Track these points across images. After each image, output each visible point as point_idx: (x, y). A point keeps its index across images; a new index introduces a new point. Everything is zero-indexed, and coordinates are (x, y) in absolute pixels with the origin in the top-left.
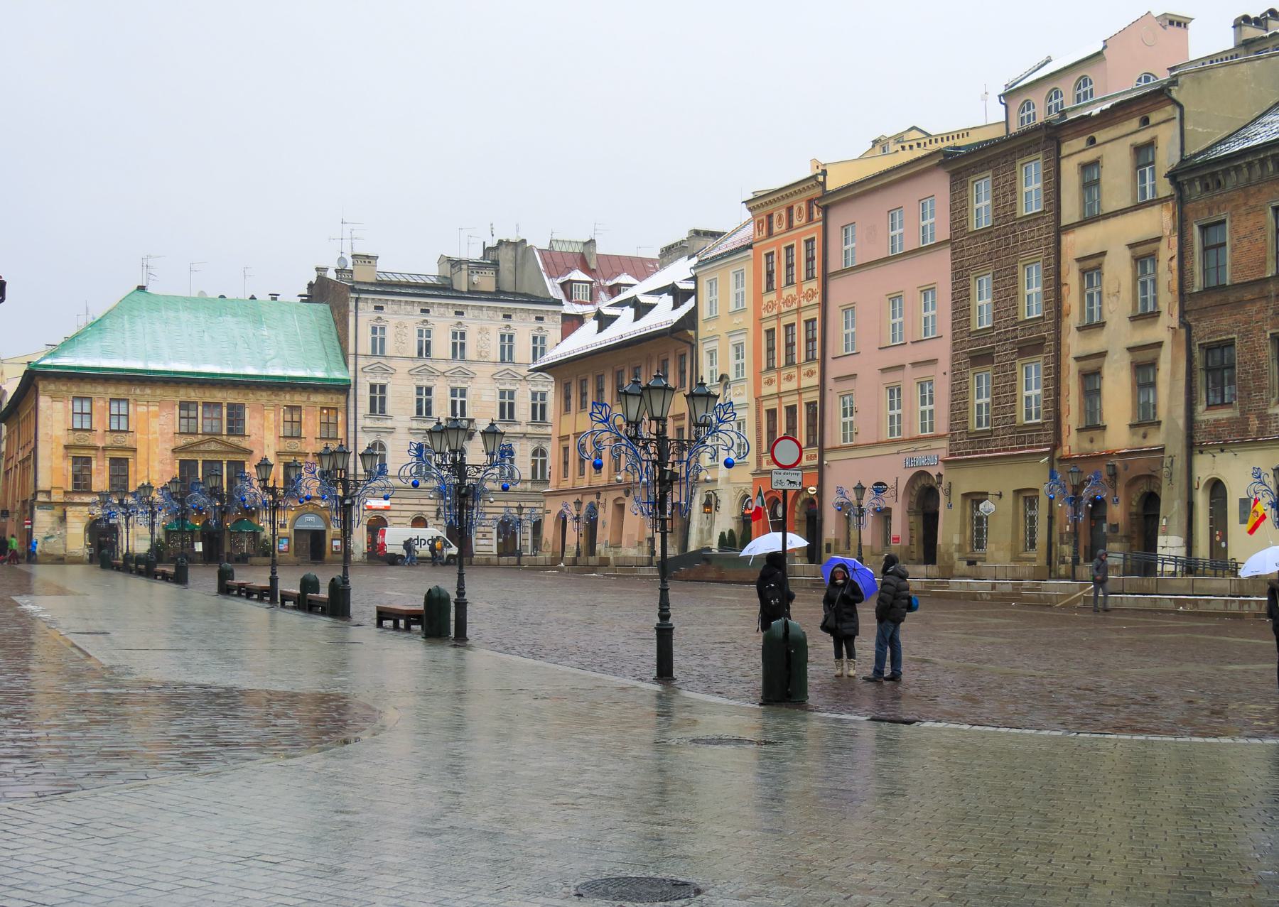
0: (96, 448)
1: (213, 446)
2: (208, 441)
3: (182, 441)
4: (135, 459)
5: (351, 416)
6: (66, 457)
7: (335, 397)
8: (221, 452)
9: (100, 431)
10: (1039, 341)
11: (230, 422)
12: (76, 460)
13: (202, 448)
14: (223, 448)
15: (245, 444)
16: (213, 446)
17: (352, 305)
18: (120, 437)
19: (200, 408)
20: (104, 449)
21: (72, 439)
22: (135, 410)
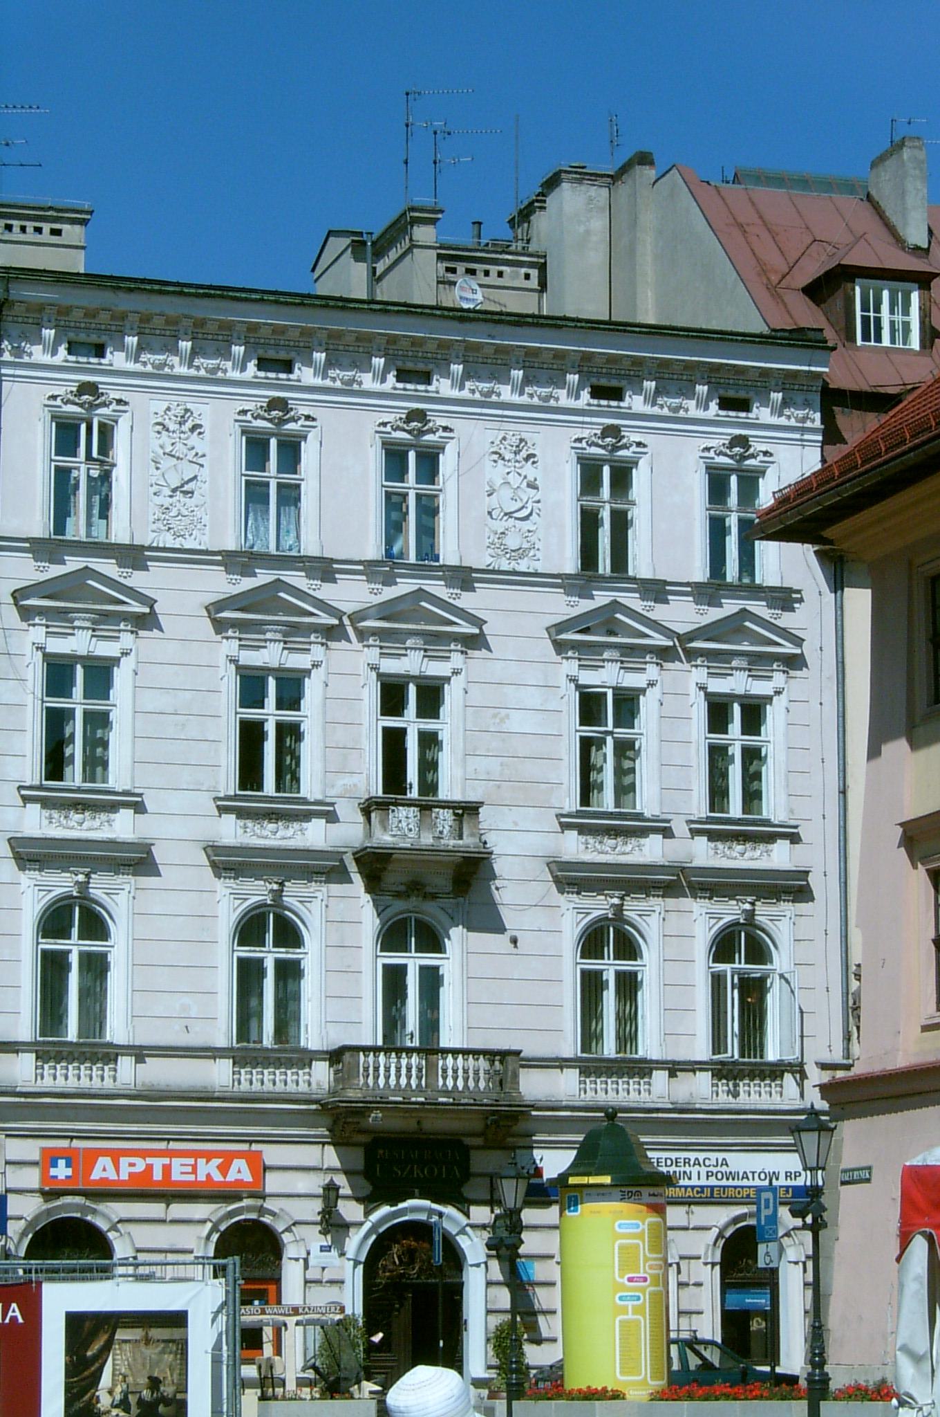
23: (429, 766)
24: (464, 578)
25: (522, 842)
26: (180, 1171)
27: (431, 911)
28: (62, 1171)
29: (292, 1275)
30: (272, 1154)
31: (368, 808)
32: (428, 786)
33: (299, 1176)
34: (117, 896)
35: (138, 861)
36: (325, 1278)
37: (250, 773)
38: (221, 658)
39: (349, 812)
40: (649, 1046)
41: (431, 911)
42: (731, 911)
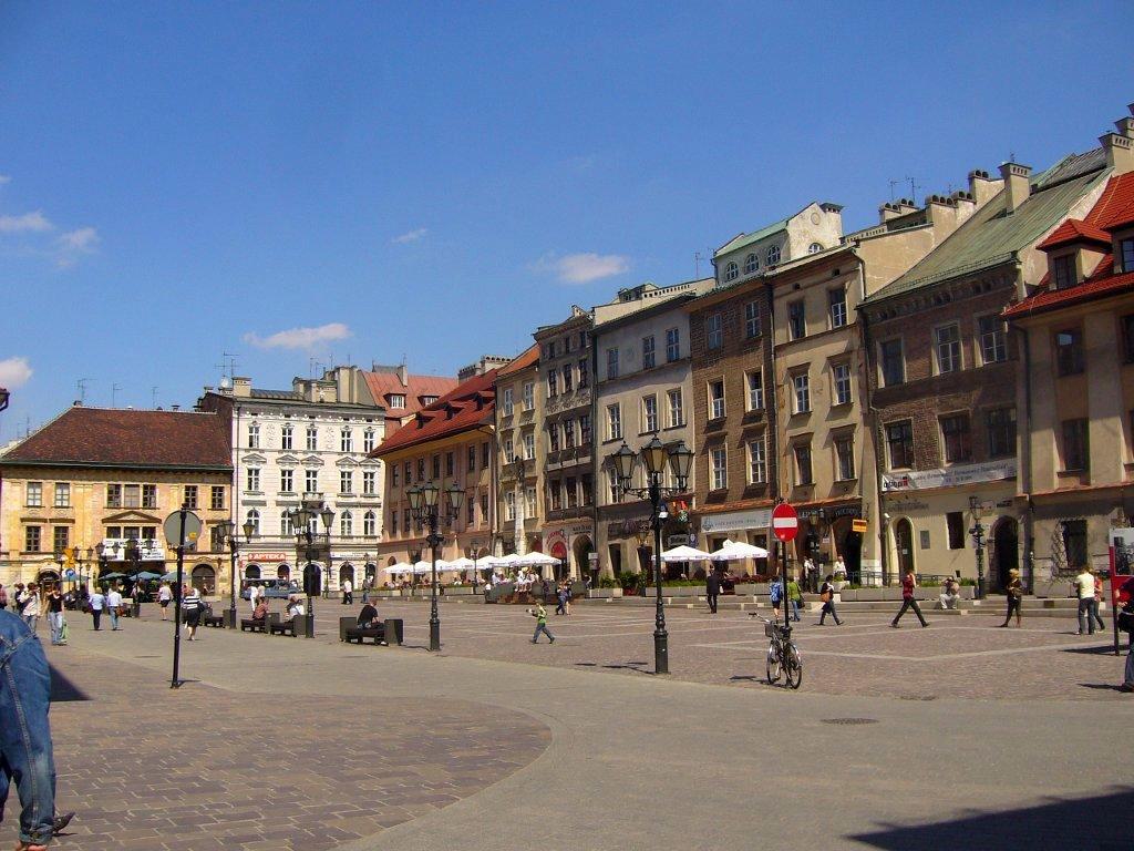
0: (45, 521)
1: (132, 517)
3: (109, 513)
5: (234, 492)
8: (137, 521)
10: (758, 426)
11: (145, 499)
12: (29, 528)
15: (155, 514)
16: (132, 517)
17: (235, 415)
20: (51, 521)
21: (26, 513)
22: (74, 492)
23: (314, 486)
24: (320, 453)
25: (330, 501)
26: (271, 558)
27: (314, 511)
28: (251, 557)
29: (291, 573)
30: (287, 553)
31: (304, 494)
32: (315, 489)
33: (291, 557)
34: (260, 509)
35: (263, 504)
36: (297, 575)
37: (283, 488)
38: (278, 469)
39: (300, 494)
40: (353, 534)
41: (314, 511)
42: (367, 510)
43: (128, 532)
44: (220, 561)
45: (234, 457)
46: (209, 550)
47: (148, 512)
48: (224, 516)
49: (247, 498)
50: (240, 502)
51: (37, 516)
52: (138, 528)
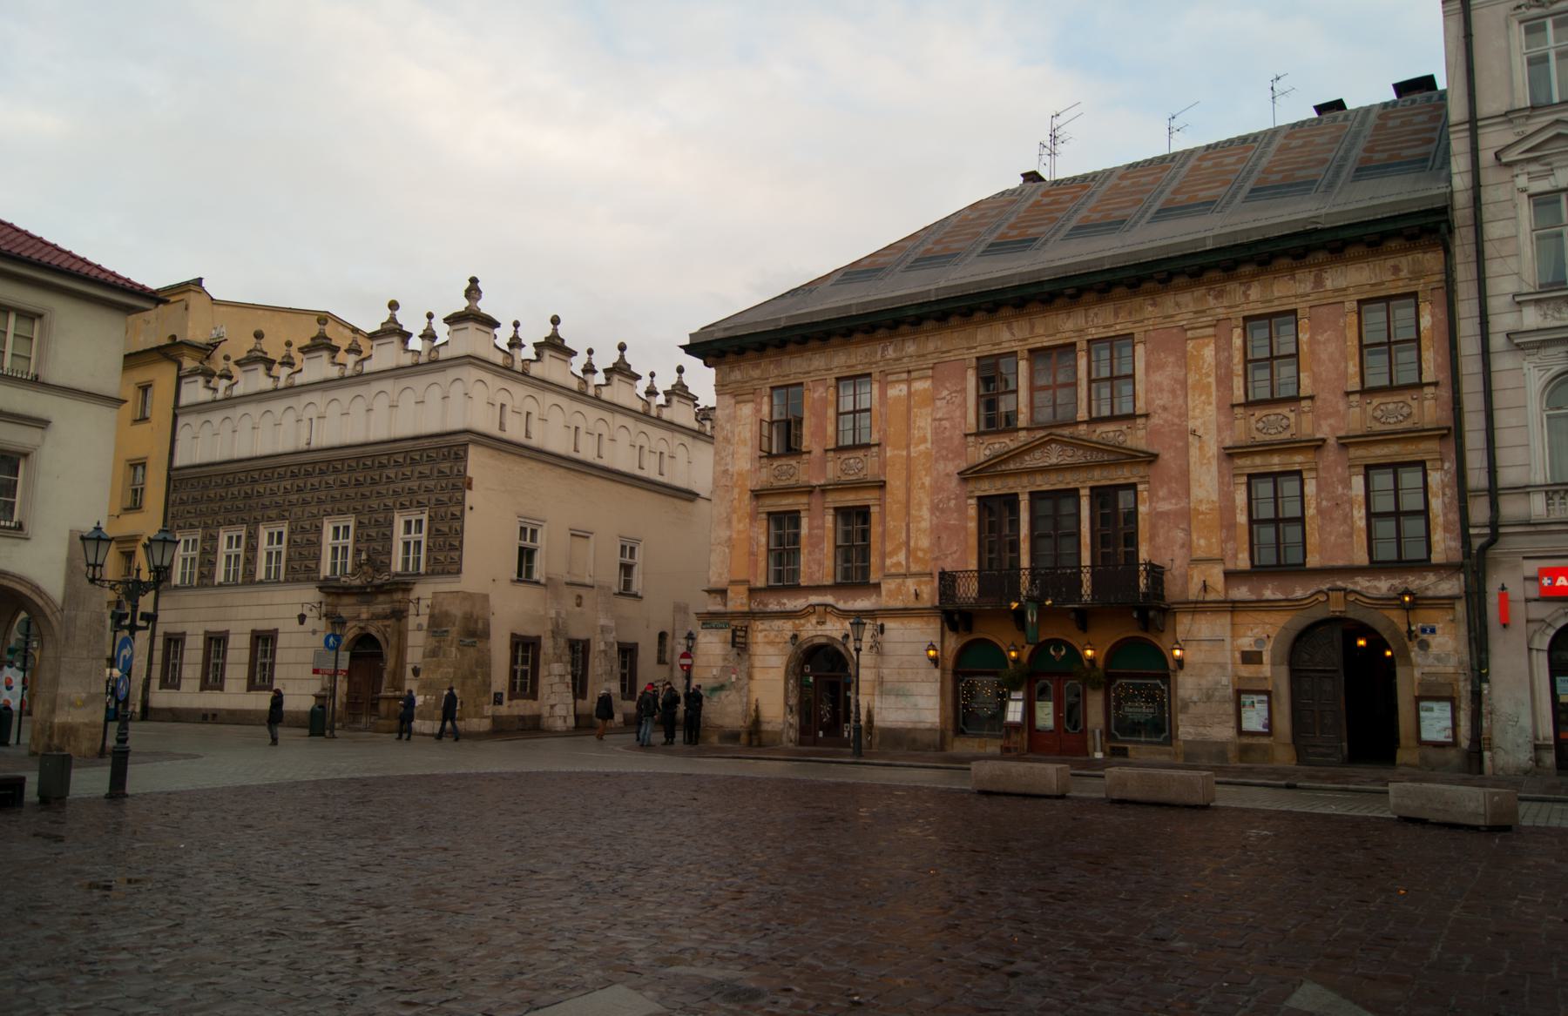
0: (809, 491)
1: (1054, 456)
2: (1043, 444)
4: (882, 505)
6: (753, 517)
7: (1405, 262)
9: (817, 451)
12: (777, 518)
13: (1030, 461)
14: (1079, 457)
15: (1137, 438)
16: (1054, 456)
18: (853, 460)
19: (1023, 366)
20: (824, 490)
21: (764, 477)
43: (1046, 507)
44: (1418, 602)
45: (1459, 164)
46: (1362, 558)
47: (1107, 431)
48: (1429, 410)
49: (1532, 318)
50: (1498, 342)
51: (792, 482)
52: (1074, 493)
